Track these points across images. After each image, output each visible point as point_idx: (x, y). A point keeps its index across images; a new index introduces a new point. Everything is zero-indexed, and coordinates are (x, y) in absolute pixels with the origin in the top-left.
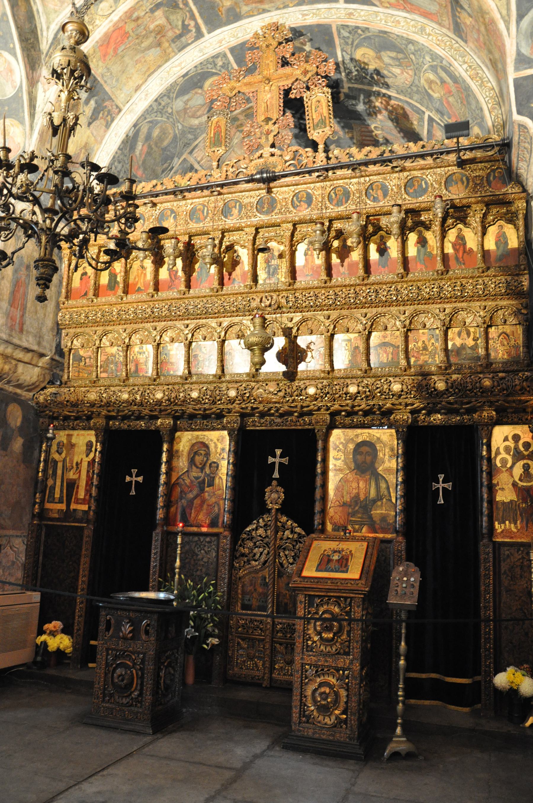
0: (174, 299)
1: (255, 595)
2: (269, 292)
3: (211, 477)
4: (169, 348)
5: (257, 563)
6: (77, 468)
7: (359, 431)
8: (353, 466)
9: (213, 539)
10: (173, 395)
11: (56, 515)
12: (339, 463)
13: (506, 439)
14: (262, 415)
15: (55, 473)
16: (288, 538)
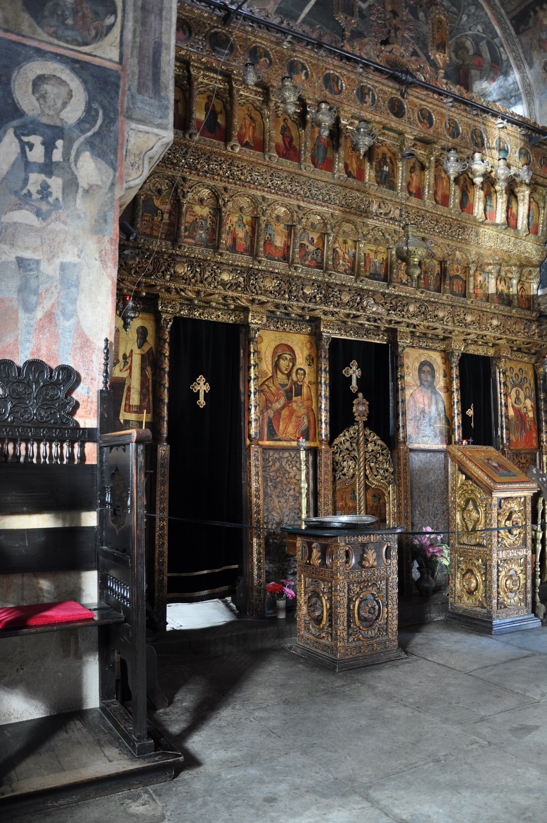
3: (298, 385)
6: (126, 363)
8: (418, 383)
16: (373, 451)
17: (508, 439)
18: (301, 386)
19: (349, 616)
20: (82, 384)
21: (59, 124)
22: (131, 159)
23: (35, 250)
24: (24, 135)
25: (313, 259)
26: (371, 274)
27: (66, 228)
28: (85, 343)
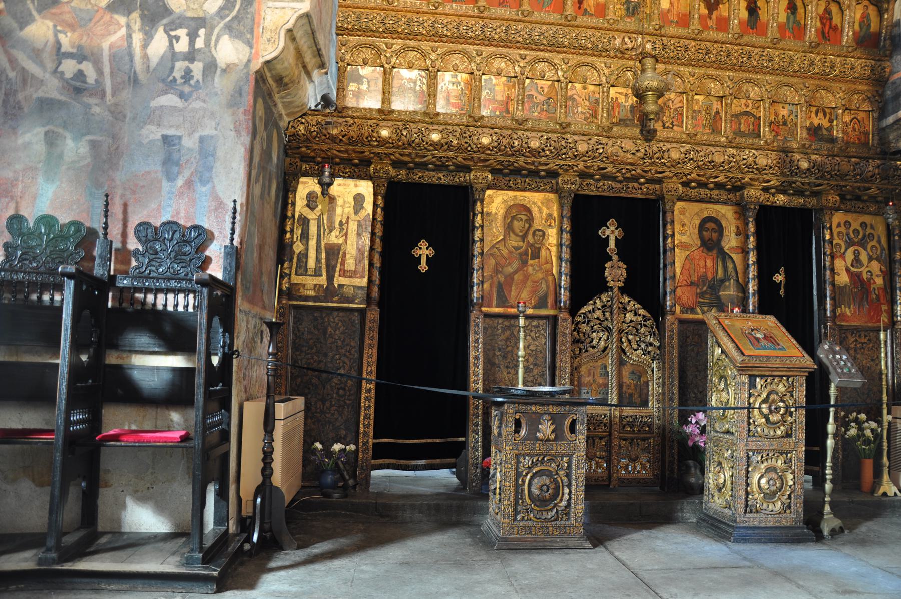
0: (511, 20)
1: (594, 386)
2: (632, 32)
3: (535, 248)
4: (494, 81)
5: (596, 350)
6: (342, 230)
7: (704, 205)
8: (699, 243)
9: (541, 322)
10: (505, 142)
11: (312, 293)
12: (684, 239)
13: (839, 225)
14: (605, 177)
15: (305, 237)
16: (631, 321)
17: (834, 311)
18: (539, 248)
19: (516, 490)
20: (215, 242)
21: (201, 14)
22: (267, 35)
23: (178, 127)
24: (172, 30)
25: (542, 110)
26: (620, 120)
27: (205, 106)
28: (220, 204)
